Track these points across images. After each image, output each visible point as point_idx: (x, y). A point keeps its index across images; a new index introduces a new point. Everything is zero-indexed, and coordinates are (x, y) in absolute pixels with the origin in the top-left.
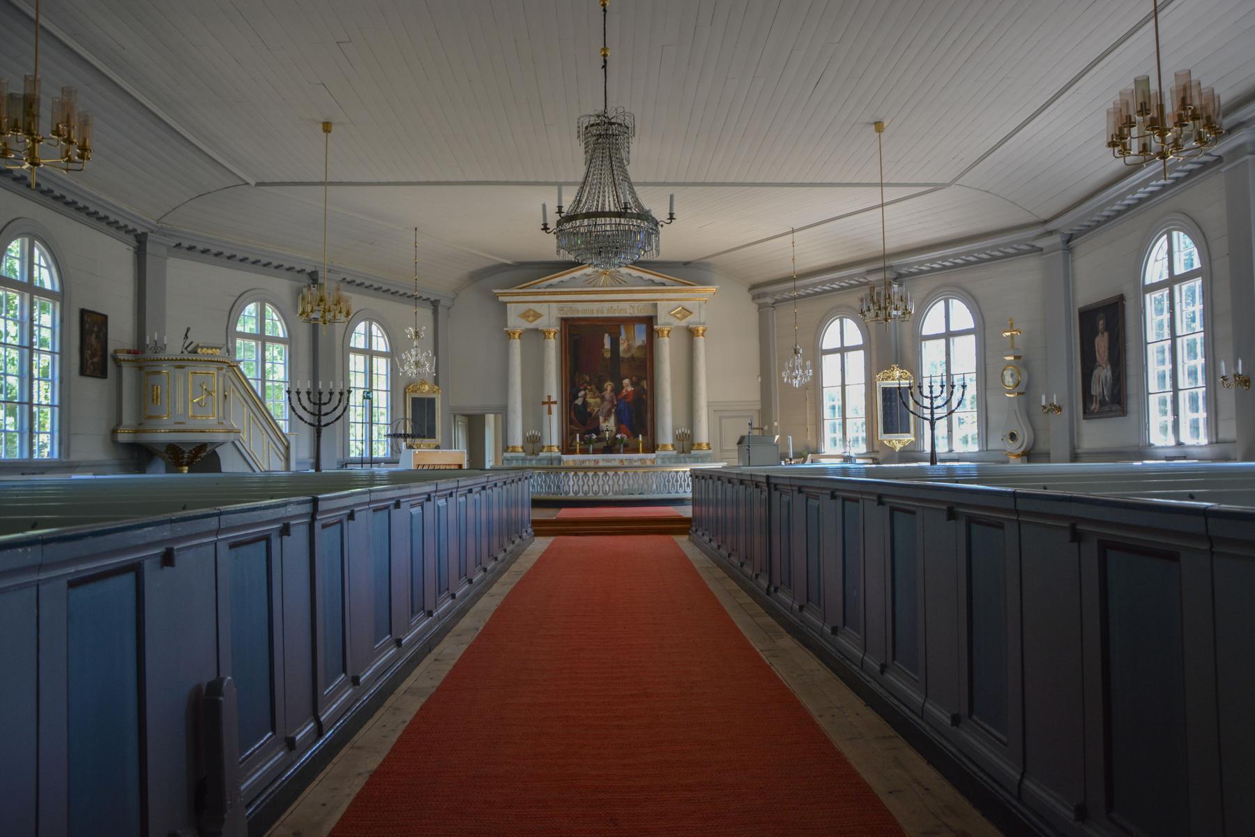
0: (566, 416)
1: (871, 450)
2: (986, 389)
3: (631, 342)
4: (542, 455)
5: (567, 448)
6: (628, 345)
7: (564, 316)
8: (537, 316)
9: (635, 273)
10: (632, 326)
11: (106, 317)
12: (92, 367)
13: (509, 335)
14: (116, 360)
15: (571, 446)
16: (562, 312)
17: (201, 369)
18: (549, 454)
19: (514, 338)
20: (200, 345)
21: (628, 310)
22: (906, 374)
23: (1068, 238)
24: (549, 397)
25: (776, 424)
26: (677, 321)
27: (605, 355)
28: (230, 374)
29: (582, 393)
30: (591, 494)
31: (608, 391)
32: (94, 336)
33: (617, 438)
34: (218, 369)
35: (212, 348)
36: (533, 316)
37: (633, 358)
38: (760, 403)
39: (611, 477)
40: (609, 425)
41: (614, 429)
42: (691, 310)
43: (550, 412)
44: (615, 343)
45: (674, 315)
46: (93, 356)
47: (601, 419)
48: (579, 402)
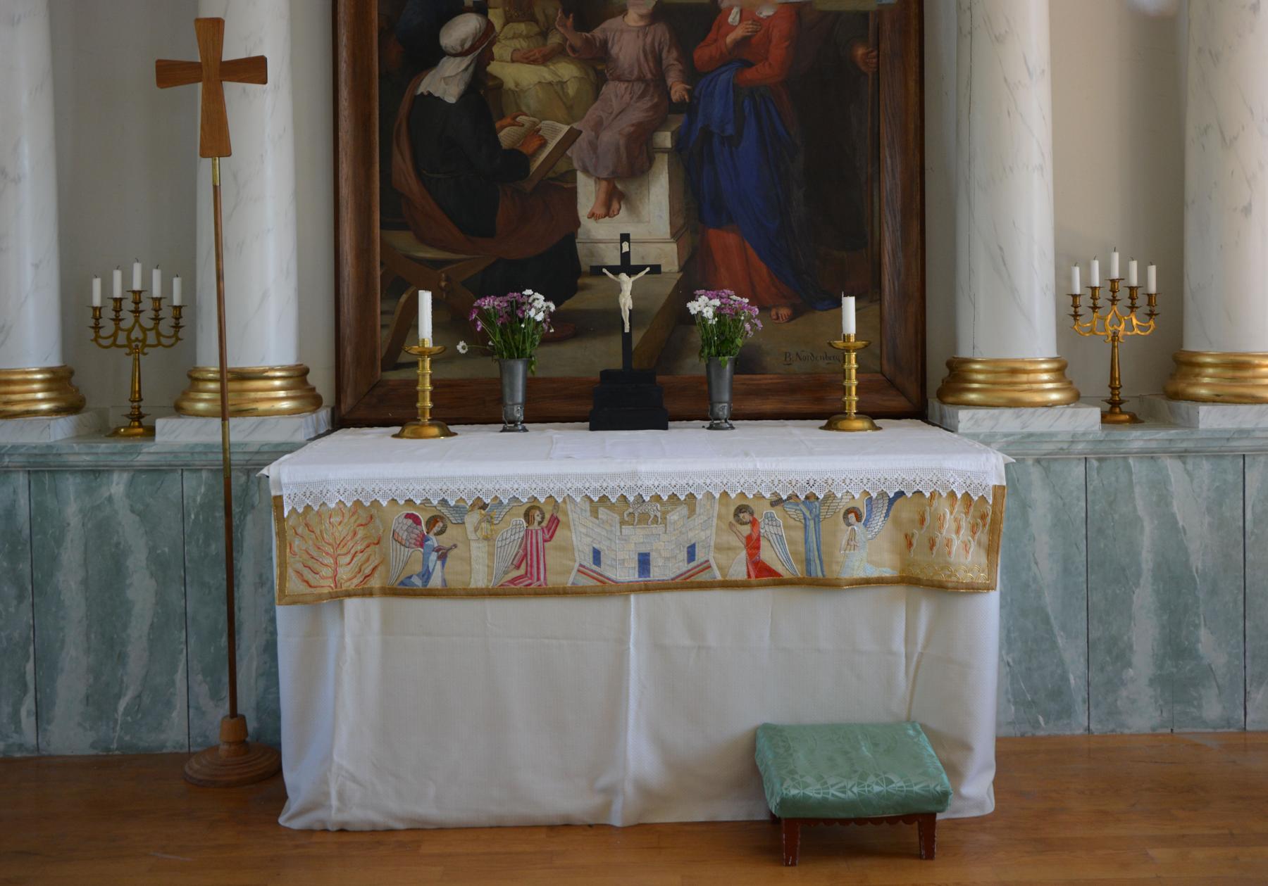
0: (363, 192)
18: (208, 432)
47: (588, 193)
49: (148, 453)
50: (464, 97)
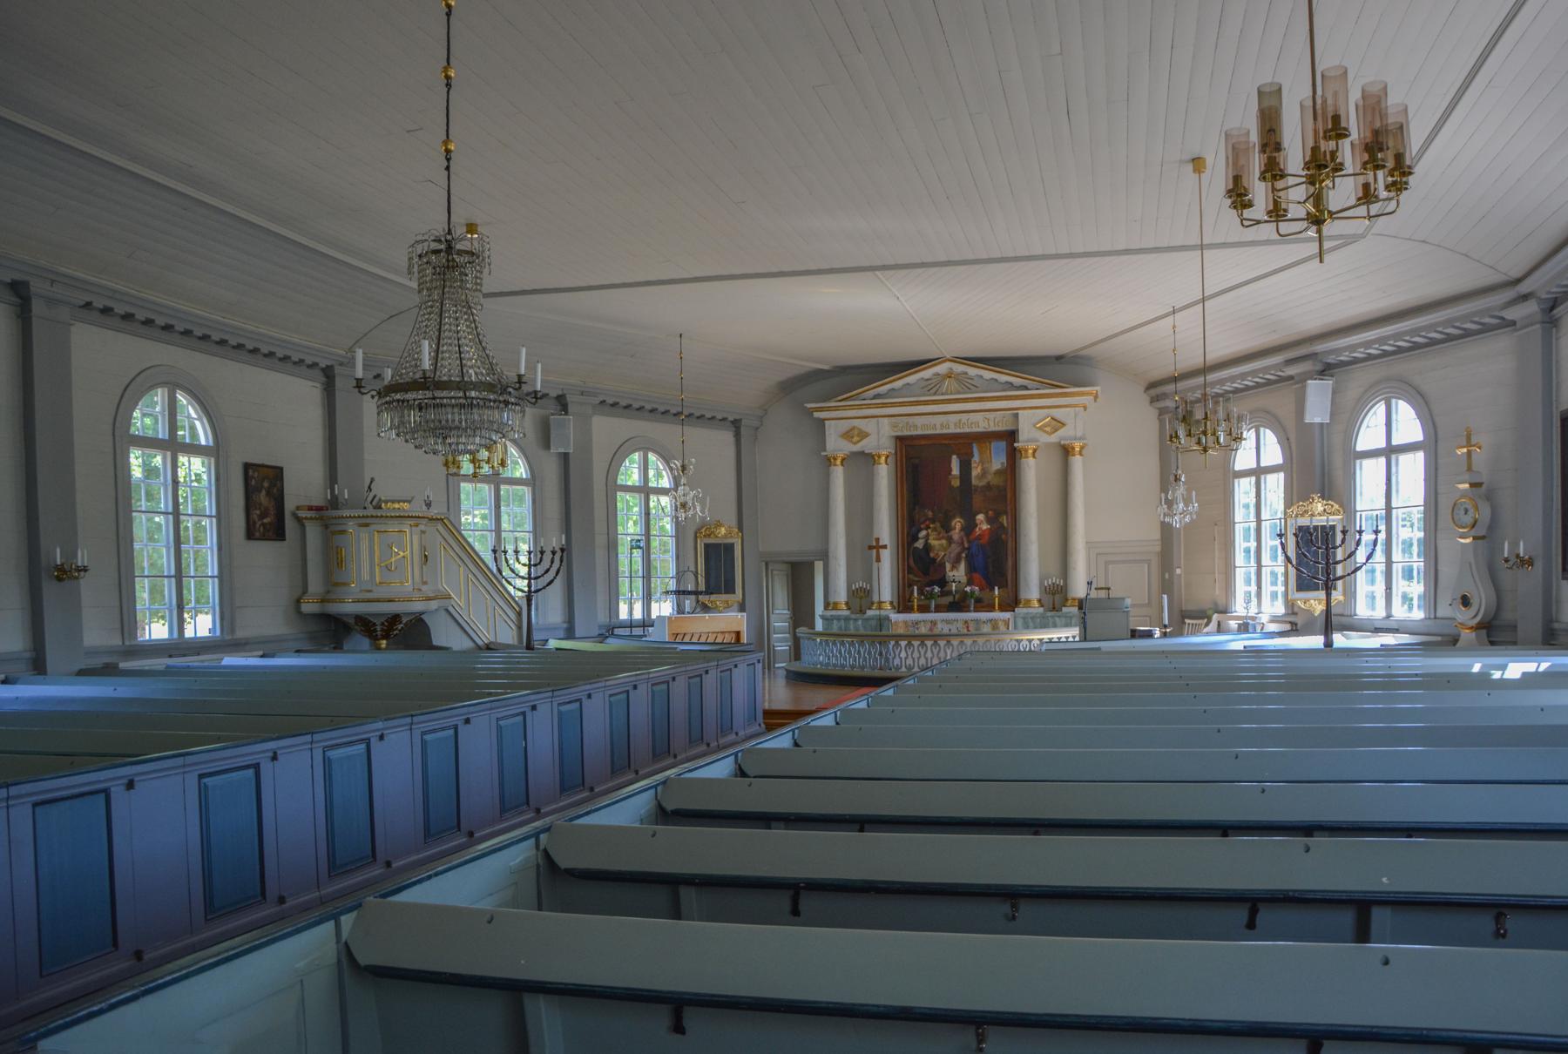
0: (903, 565)
1: (1290, 612)
2: (1436, 530)
3: (986, 465)
4: (870, 613)
5: (904, 605)
6: (983, 469)
7: (899, 434)
8: (864, 435)
9: (988, 375)
10: (988, 444)
11: (281, 469)
12: (262, 529)
13: (829, 461)
14: (299, 520)
15: (909, 601)
16: (895, 429)
17: (393, 527)
18: (877, 612)
19: (835, 465)
20: (383, 498)
21: (981, 424)
22: (1332, 506)
23: (1551, 304)
24: (877, 540)
25: (1178, 571)
26: (1045, 436)
27: (952, 483)
28: (440, 527)
29: (923, 533)
30: (904, 669)
31: (957, 531)
32: (264, 492)
33: (966, 592)
34: (411, 525)
35: (399, 502)
36: (858, 436)
37: (988, 487)
38: (1160, 543)
39: (955, 647)
40: (958, 574)
41: (964, 579)
42: (1063, 420)
43: (878, 560)
44: (966, 466)
45: (1040, 428)
46: (263, 516)
47: (948, 566)
48: (920, 544)
49: (866, 616)
50: (924, 546)
